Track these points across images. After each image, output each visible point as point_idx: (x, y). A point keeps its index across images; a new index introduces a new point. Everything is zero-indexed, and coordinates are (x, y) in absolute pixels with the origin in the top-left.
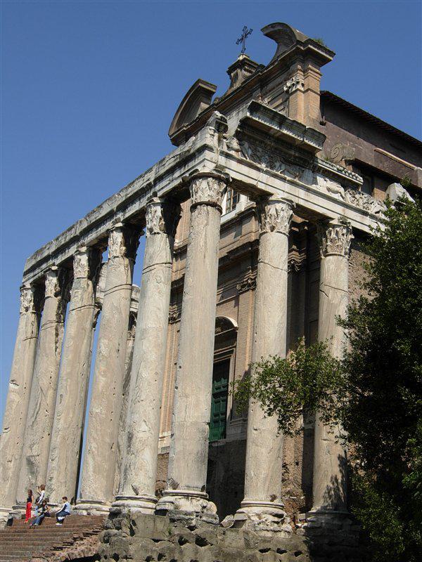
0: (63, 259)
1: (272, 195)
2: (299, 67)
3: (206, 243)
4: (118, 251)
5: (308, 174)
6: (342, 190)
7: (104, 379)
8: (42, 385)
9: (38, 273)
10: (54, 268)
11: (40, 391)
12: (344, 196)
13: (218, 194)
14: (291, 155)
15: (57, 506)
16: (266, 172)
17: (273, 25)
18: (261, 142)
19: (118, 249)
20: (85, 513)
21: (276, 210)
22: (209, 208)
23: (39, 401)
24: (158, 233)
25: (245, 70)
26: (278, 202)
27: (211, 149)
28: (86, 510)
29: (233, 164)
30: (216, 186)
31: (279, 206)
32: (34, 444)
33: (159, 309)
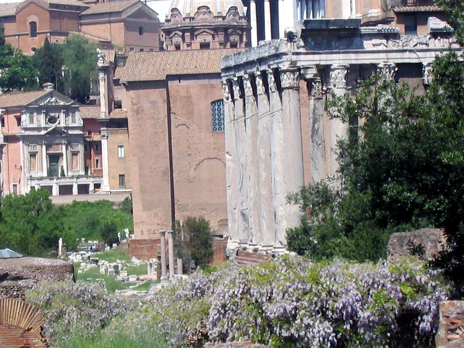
1: (331, 65)
3: (290, 112)
5: (357, 40)
6: (384, 41)
12: (386, 44)
13: (294, 80)
14: (342, 35)
15: (256, 245)
16: (326, 53)
19: (261, 88)
22: (290, 90)
24: (274, 92)
26: (336, 69)
27: (286, 54)
29: (302, 57)
30: (292, 76)
31: (336, 72)
32: (243, 202)
33: (281, 139)
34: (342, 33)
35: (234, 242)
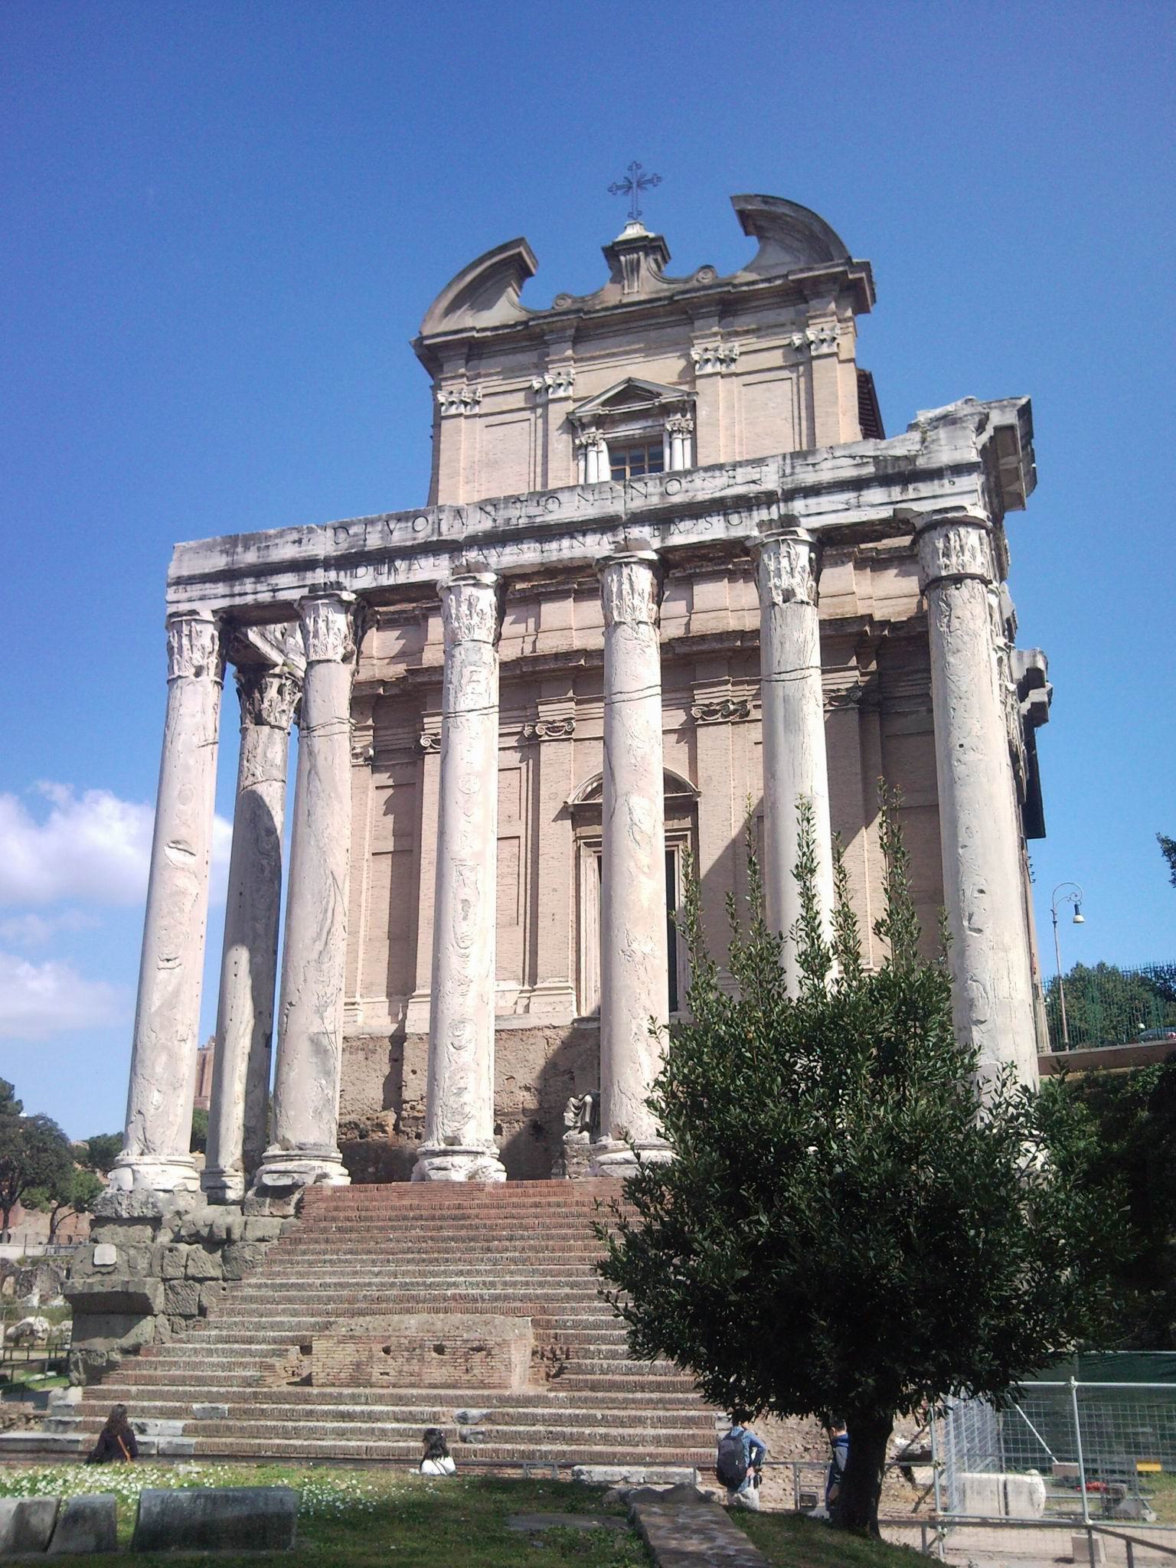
0: (386, 580)
2: (833, 306)
4: (644, 610)
8: (335, 868)
9: (254, 593)
10: (347, 596)
11: (330, 881)
17: (766, 199)
25: (656, 261)
35: (172, 1163)
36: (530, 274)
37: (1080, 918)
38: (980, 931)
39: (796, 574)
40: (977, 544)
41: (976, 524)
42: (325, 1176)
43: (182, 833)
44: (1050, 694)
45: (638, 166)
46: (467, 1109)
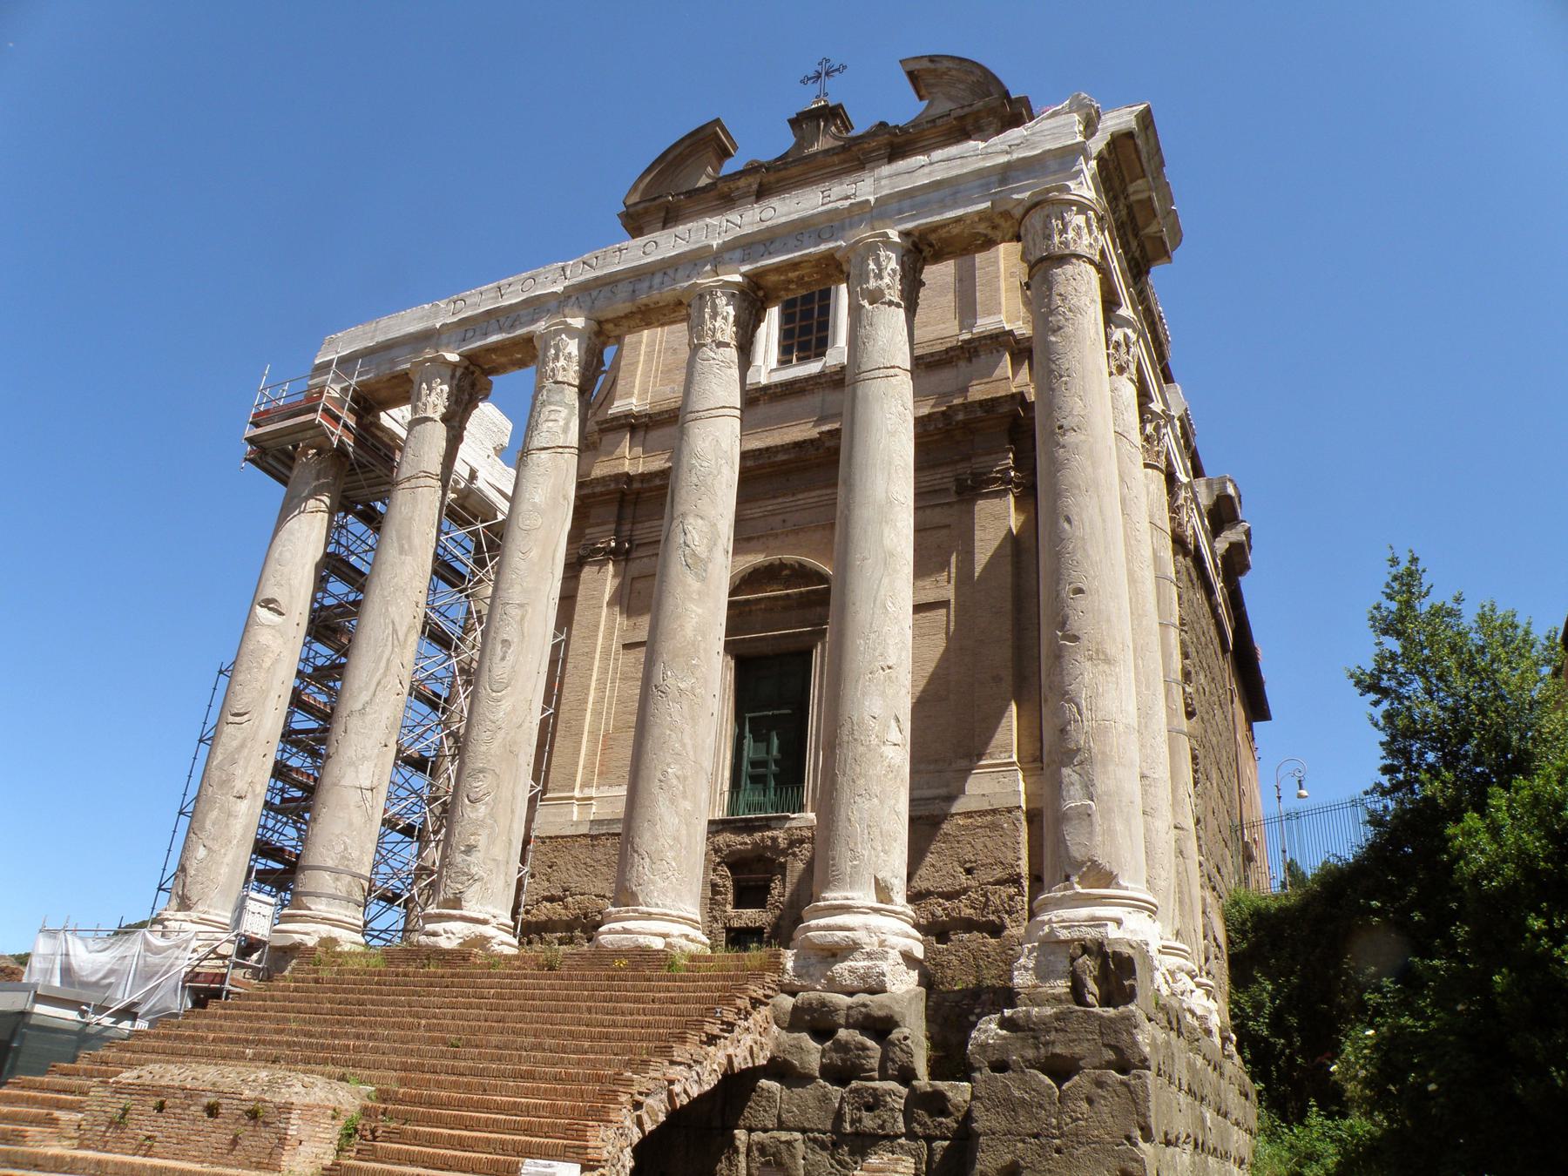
7: (700, 611)
8: (397, 620)
15: (485, 922)
17: (932, 59)
18: (1116, 198)
20: (658, 944)
21: (1126, 336)
23: (387, 653)
24: (898, 305)
28: (664, 936)
34: (1134, 244)
36: (730, 155)
37: (1304, 793)
38: (1075, 638)
39: (885, 274)
40: (1083, 224)
41: (1083, 208)
42: (333, 941)
43: (269, 592)
44: (1248, 533)
45: (828, 61)
46: (474, 870)
